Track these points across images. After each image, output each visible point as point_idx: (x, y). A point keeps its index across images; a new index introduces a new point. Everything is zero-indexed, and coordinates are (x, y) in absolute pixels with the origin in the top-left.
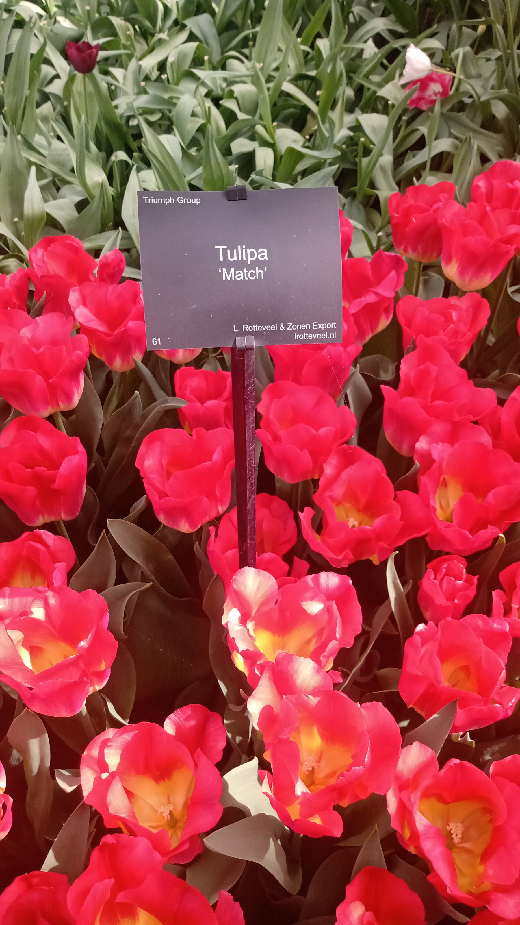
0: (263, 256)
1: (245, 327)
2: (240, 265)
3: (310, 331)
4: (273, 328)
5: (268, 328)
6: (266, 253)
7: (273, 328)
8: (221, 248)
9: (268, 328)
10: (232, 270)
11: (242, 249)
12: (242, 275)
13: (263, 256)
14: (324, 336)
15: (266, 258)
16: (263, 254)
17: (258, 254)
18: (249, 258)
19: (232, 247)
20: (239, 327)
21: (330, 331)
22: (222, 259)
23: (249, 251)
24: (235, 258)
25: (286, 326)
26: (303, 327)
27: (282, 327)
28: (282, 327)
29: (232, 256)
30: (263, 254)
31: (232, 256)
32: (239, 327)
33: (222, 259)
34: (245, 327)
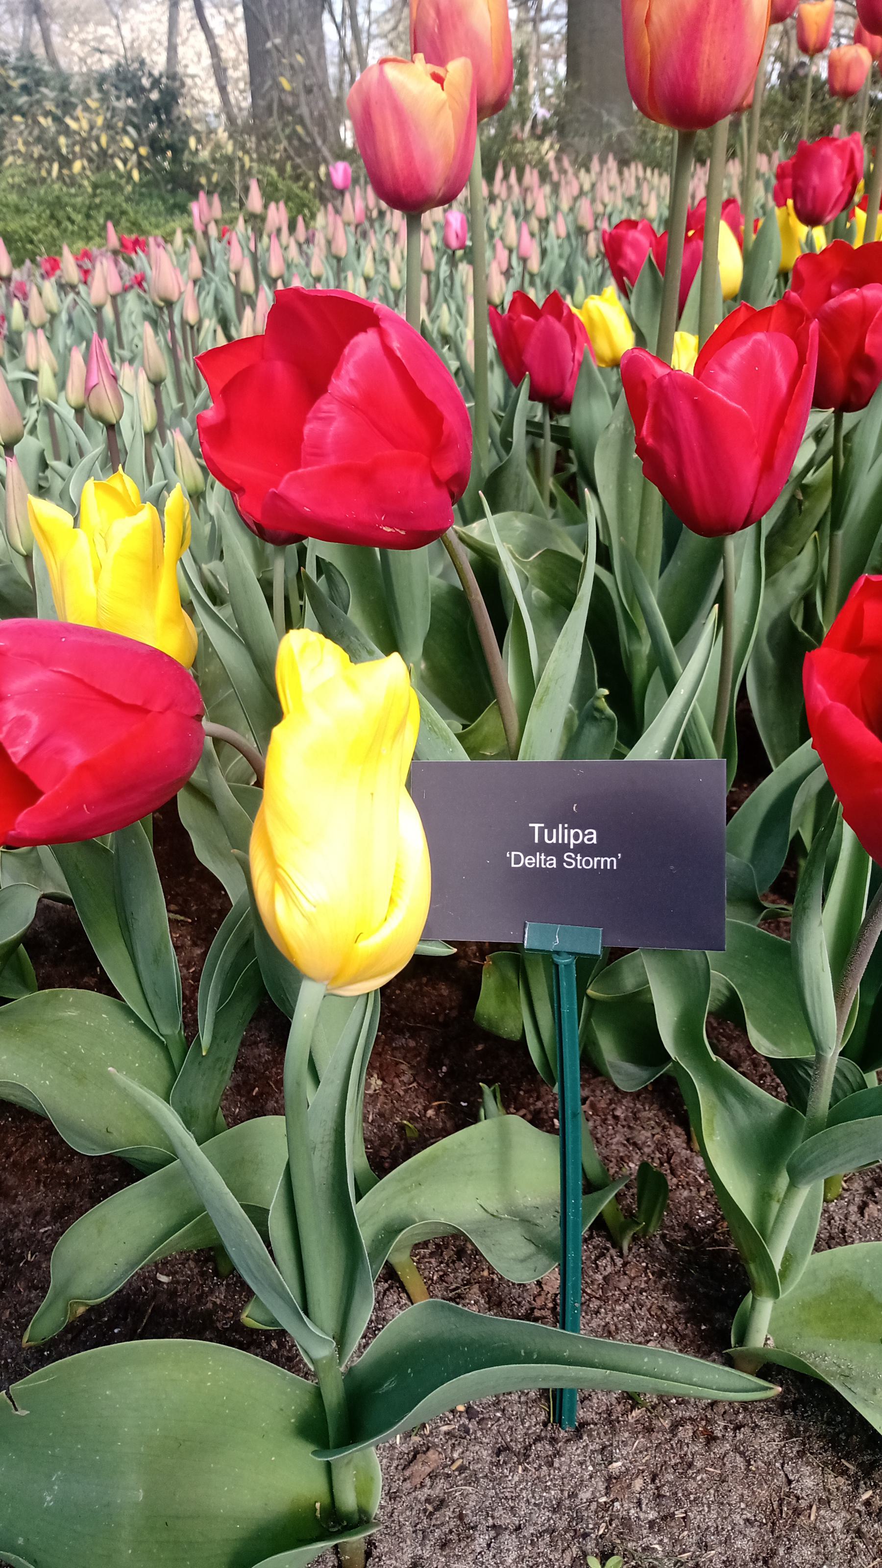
0: (590, 839)
6: (594, 836)
11: (564, 828)
13: (590, 839)
15: (595, 841)
16: (592, 837)
17: (584, 835)
18: (572, 841)
19: (551, 825)
22: (536, 841)
23: (572, 832)
24: (554, 841)
29: (550, 838)
30: (592, 837)
31: (550, 838)
33: (536, 841)
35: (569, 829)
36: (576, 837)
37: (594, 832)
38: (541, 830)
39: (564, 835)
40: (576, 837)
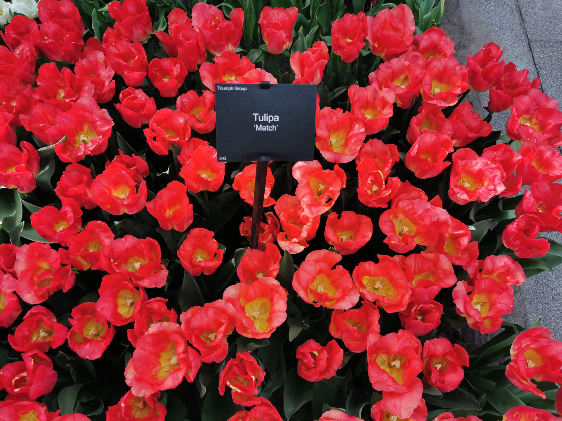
2: (265, 123)
8: (256, 115)
10: (261, 126)
12: (266, 128)
15: (278, 120)
16: (277, 118)
19: (261, 114)
22: (256, 120)
23: (270, 117)
24: (262, 120)
29: (261, 119)
30: (277, 118)
31: (261, 119)
33: (256, 120)
35: (268, 115)
36: (271, 118)
37: (278, 117)
38: (258, 116)
39: (266, 118)
40: (271, 118)
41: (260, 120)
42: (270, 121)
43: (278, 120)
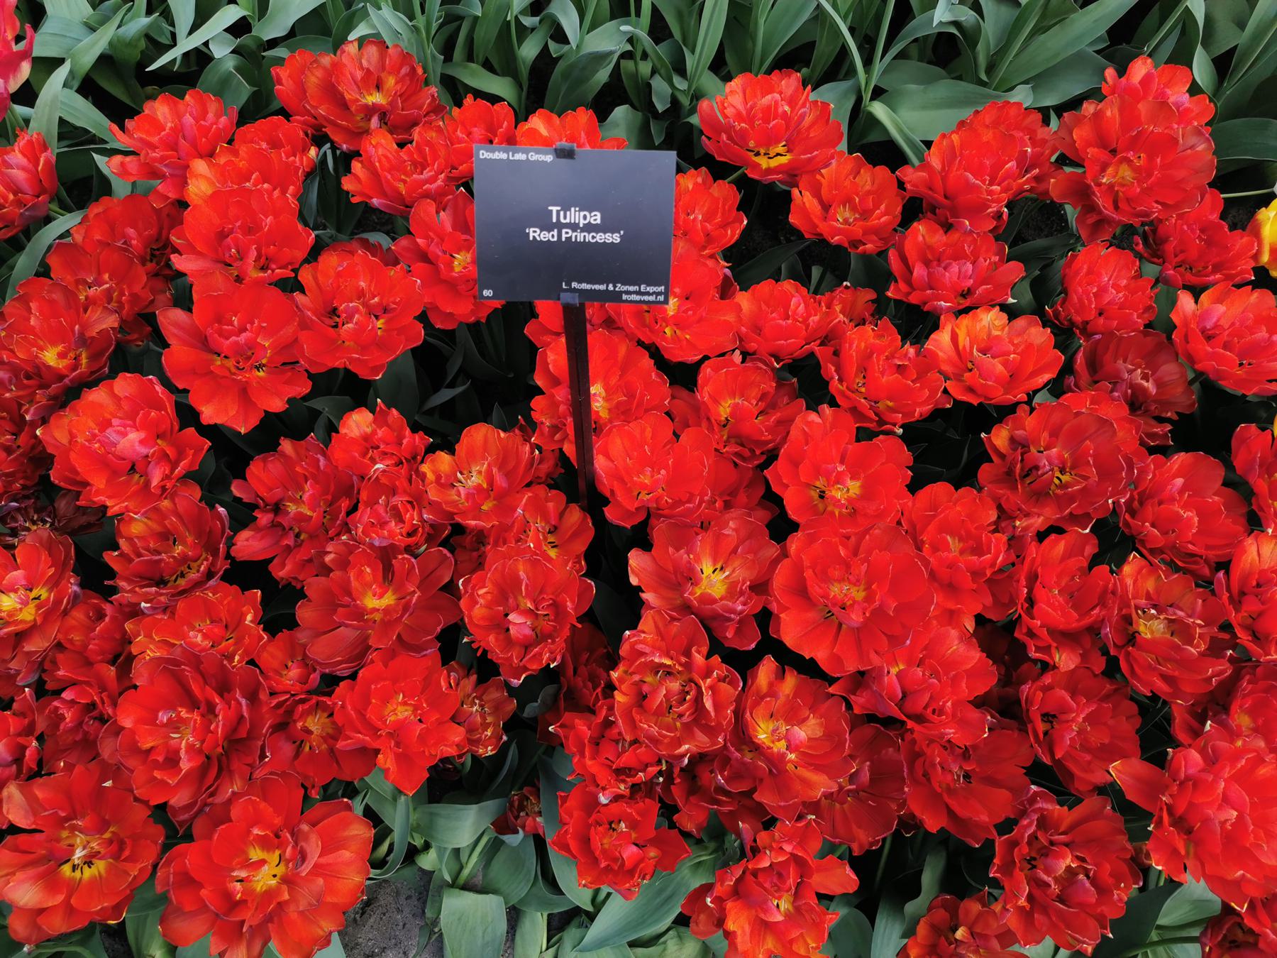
1: (574, 285)
2: (574, 227)
3: (639, 293)
4: (602, 287)
5: (597, 287)
7: (602, 287)
8: (554, 209)
9: (597, 287)
14: (652, 298)
15: (599, 221)
16: (596, 218)
19: (566, 209)
20: (569, 284)
21: (658, 294)
23: (582, 214)
25: (615, 287)
26: (631, 288)
27: (611, 287)
28: (611, 287)
30: (596, 218)
32: (569, 284)
34: (574, 285)
36: (585, 217)
37: (598, 214)
38: (558, 212)
40: (585, 217)
41: (562, 220)
42: (582, 223)
43: (599, 221)
